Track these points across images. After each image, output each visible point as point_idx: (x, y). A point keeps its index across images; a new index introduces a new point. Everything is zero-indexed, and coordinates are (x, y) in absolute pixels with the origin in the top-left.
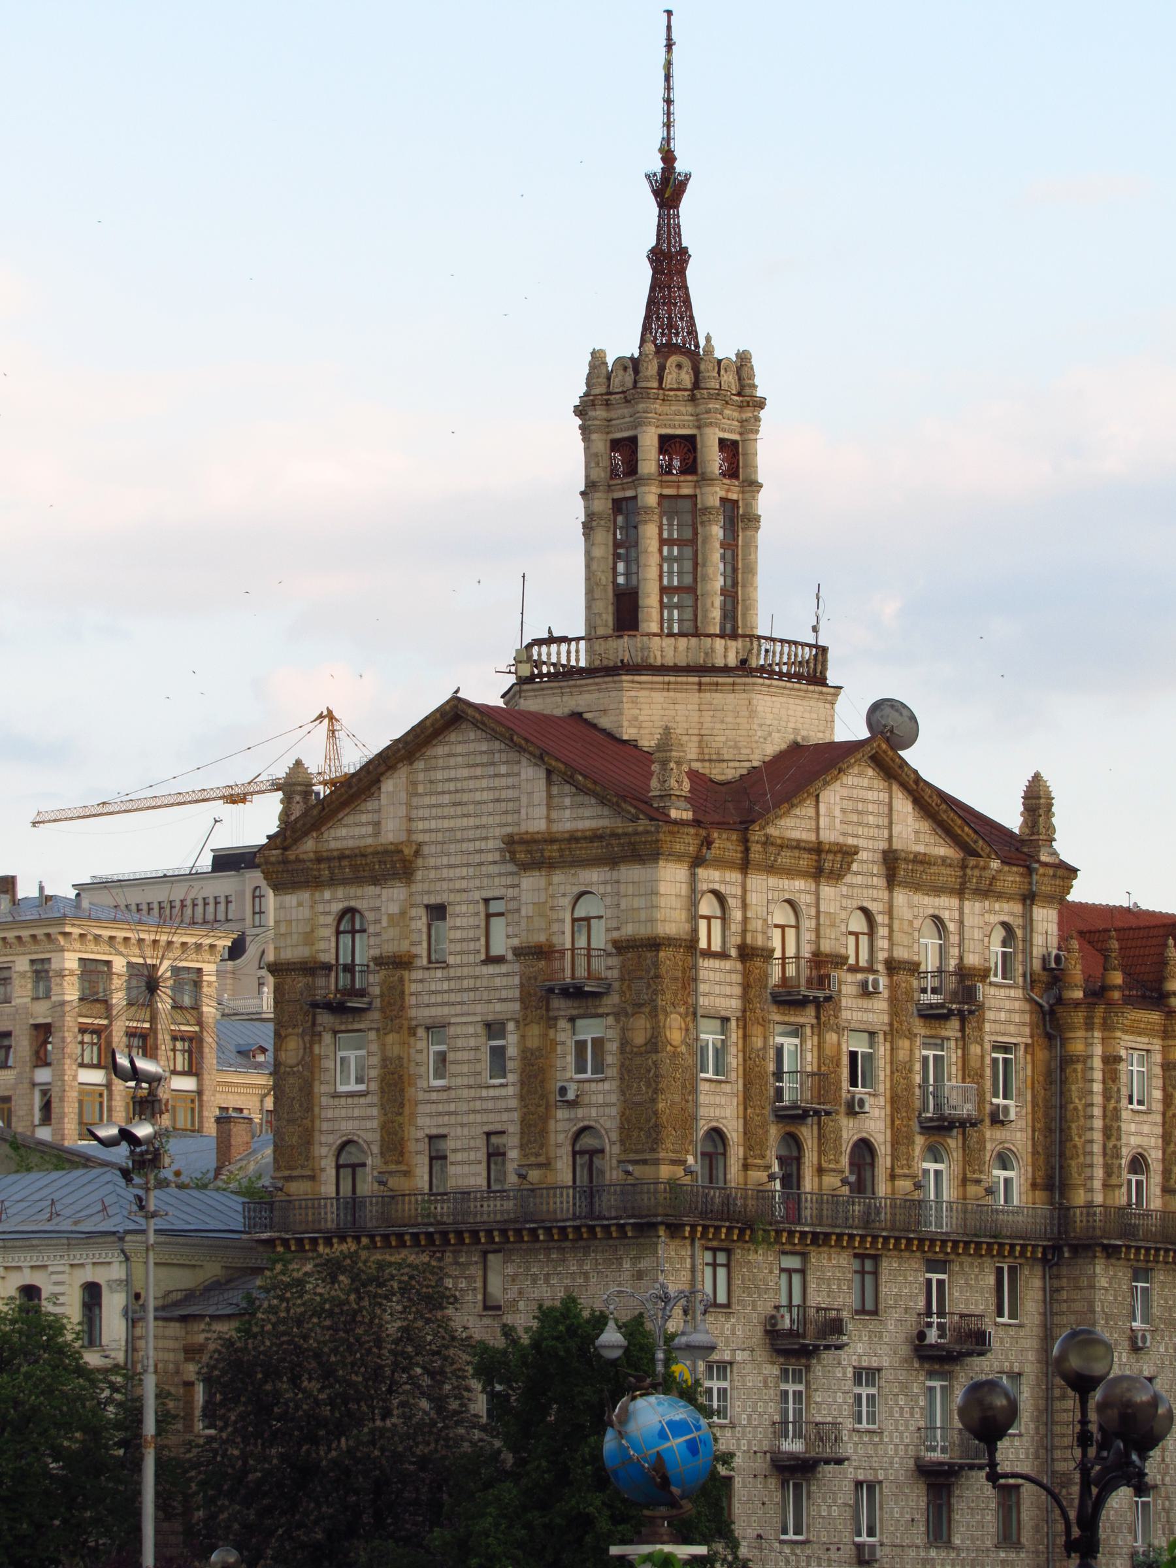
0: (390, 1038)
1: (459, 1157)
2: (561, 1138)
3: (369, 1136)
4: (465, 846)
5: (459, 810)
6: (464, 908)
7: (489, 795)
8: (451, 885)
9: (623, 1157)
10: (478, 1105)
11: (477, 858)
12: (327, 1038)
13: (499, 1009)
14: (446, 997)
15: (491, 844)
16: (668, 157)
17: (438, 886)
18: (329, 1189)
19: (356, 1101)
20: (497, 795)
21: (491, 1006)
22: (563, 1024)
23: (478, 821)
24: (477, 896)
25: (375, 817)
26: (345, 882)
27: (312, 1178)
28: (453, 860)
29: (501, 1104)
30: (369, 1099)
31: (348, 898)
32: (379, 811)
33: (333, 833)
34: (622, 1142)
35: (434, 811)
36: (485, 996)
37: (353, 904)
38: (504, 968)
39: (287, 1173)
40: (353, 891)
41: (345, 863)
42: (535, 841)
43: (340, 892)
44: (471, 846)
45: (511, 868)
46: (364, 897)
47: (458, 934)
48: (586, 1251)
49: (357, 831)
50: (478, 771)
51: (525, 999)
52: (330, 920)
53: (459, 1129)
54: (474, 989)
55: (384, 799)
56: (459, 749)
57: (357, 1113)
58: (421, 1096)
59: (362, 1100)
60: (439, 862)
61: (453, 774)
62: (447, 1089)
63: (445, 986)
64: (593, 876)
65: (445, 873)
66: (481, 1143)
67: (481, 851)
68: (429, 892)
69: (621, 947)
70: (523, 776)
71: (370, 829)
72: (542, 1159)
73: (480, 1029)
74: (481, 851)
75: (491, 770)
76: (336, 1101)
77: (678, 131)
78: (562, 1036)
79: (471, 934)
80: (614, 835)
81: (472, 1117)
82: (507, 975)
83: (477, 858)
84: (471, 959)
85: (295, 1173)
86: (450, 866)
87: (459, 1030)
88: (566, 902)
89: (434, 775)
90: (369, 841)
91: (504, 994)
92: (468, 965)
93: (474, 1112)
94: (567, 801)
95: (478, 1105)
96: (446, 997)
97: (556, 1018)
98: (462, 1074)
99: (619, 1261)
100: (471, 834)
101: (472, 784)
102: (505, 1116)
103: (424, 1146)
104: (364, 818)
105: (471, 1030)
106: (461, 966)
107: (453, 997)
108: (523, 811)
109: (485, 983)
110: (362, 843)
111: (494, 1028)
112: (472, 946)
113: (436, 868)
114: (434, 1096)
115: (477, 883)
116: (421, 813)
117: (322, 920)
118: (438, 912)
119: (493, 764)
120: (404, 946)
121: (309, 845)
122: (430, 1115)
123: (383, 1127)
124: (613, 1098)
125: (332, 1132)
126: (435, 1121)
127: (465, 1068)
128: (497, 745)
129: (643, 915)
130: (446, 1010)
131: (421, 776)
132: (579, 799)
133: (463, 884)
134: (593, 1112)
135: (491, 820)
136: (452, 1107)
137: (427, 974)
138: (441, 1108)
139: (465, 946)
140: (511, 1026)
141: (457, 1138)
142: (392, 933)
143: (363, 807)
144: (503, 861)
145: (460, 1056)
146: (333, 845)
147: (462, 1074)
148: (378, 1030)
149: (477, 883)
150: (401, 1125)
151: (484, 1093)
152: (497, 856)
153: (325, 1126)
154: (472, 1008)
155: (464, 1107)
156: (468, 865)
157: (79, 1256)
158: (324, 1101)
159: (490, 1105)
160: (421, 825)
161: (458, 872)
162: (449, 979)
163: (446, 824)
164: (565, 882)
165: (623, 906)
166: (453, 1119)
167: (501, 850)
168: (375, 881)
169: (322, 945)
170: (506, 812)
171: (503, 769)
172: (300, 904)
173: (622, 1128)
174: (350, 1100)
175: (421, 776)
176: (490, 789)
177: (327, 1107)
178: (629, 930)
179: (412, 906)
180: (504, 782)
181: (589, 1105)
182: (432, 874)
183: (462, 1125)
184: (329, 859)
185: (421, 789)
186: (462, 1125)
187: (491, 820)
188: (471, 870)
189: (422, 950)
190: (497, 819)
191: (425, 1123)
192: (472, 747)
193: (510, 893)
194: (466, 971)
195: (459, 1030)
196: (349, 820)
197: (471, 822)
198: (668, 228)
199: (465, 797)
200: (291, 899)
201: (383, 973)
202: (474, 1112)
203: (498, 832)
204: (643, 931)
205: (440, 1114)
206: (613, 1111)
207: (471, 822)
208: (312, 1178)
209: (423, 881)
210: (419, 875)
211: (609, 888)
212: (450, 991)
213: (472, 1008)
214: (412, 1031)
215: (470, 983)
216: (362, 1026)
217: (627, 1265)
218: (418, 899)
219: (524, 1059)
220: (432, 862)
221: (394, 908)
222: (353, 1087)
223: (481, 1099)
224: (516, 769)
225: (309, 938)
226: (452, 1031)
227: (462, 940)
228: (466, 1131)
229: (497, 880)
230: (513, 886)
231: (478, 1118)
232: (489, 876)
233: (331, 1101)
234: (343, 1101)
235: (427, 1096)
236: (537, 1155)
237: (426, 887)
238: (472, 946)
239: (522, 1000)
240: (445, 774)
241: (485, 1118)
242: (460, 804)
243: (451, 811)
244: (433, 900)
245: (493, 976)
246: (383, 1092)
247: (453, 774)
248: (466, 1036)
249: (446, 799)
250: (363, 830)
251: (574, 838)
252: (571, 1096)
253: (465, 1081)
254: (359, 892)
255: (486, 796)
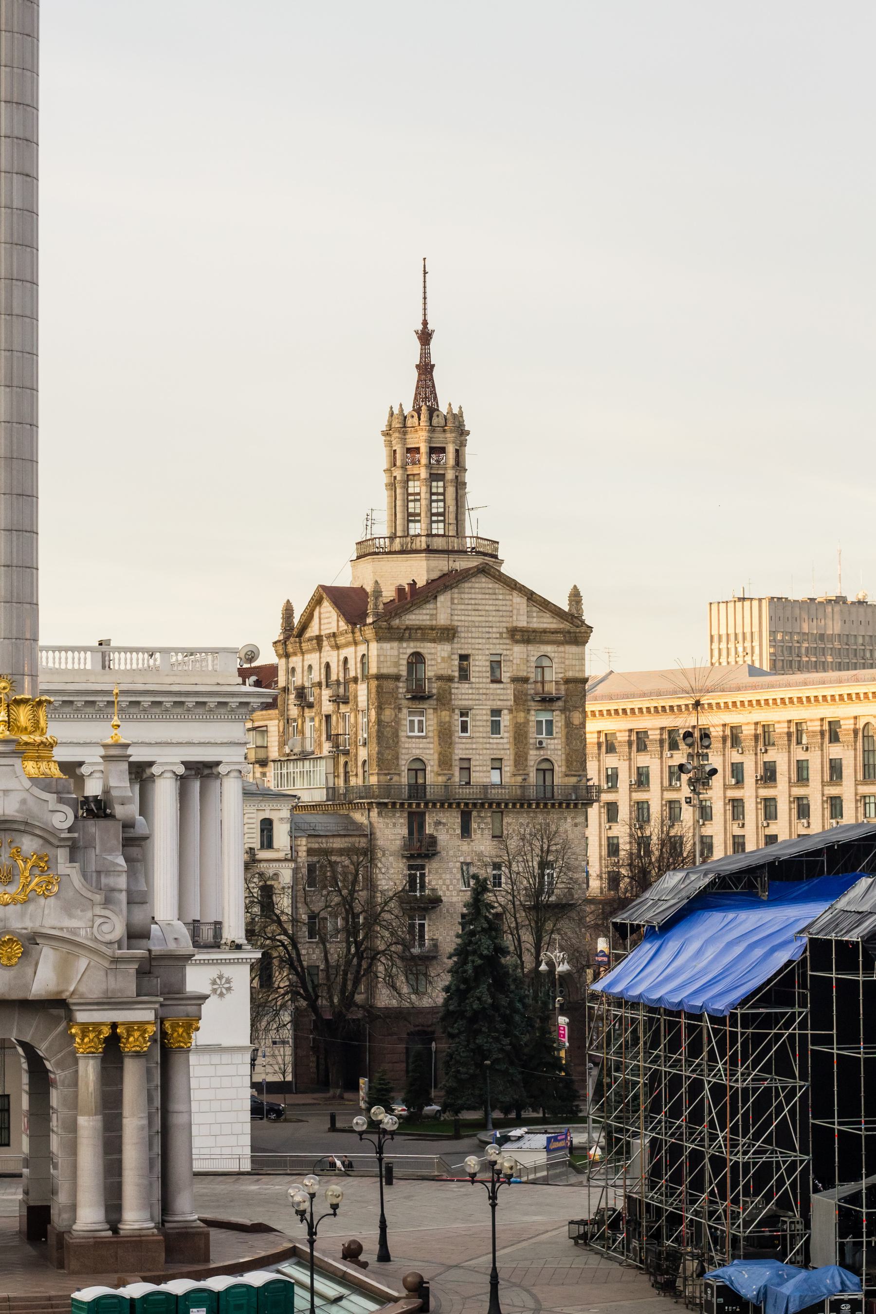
0: (444, 713)
1: (478, 768)
2: (532, 763)
3: (428, 757)
4: (480, 629)
5: (477, 613)
6: (480, 657)
7: (494, 608)
8: (473, 646)
9: (568, 773)
10: (488, 746)
11: (487, 635)
12: (405, 711)
13: (498, 704)
14: (470, 696)
15: (495, 630)
16: (425, 323)
17: (466, 646)
18: (404, 780)
19: (421, 740)
20: (497, 608)
21: (495, 703)
22: (533, 712)
23: (487, 619)
24: (487, 652)
25: (432, 612)
26: (417, 640)
27: (399, 775)
28: (474, 635)
29: (501, 746)
30: (428, 740)
31: (416, 647)
32: (436, 609)
33: (407, 617)
34: (568, 767)
35: (463, 612)
36: (492, 697)
37: (419, 650)
38: (501, 686)
39: (386, 772)
40: (418, 644)
41: (420, 631)
42: (528, 631)
43: (412, 644)
44: (484, 630)
45: (508, 641)
46: (427, 648)
47: (477, 669)
48: (548, 813)
49: (421, 617)
50: (487, 596)
51: (516, 698)
52: (406, 656)
53: (478, 757)
54: (486, 694)
55: (439, 604)
56: (477, 585)
57: (421, 746)
58: (457, 740)
59: (424, 740)
60: (466, 635)
61: (473, 596)
62: (470, 738)
63: (470, 691)
64: (548, 649)
65: (470, 640)
66: (489, 763)
67: (489, 633)
68: (461, 649)
69: (567, 681)
70: (515, 600)
71: (428, 617)
72: (525, 772)
73: (489, 712)
74: (489, 633)
75: (494, 597)
76: (410, 740)
77: (428, 312)
78: (533, 718)
79: (484, 669)
80: (569, 632)
81: (485, 751)
82: (503, 689)
83: (487, 635)
84: (484, 680)
85: (390, 772)
86: (472, 638)
87: (478, 712)
88: (535, 658)
89: (463, 596)
90: (428, 623)
91: (502, 697)
92: (483, 683)
93: (486, 749)
94: (535, 614)
95: (488, 746)
96: (470, 696)
97: (529, 710)
98: (479, 732)
99: (566, 819)
100: (484, 624)
101: (484, 602)
102: (502, 752)
103: (457, 763)
104: (424, 612)
105: (484, 712)
106: (479, 683)
107: (474, 697)
108: (515, 617)
109: (491, 691)
110: (424, 623)
111: (496, 712)
112: (484, 674)
113: (465, 638)
114: (464, 740)
115: (487, 646)
116: (456, 612)
117: (401, 656)
118: (464, 658)
119: (495, 594)
120: (450, 672)
121: (396, 622)
122: (462, 749)
123: (440, 754)
124: (560, 747)
125: (408, 754)
126: (464, 752)
127: (481, 729)
128: (497, 586)
129: (577, 668)
130: (470, 702)
131: (456, 596)
132: (541, 614)
133: (480, 646)
134: (549, 752)
135: (494, 619)
136: (474, 746)
137: (460, 685)
138: (467, 746)
139: (481, 675)
140: (505, 712)
141: (476, 760)
142: (443, 665)
143: (424, 606)
144: (501, 638)
145: (478, 723)
146: (407, 622)
147: (479, 732)
148: (434, 709)
149: (487, 646)
150: (450, 753)
151: (491, 741)
152: (498, 636)
153: (404, 751)
154: (484, 702)
155: (481, 746)
156: (482, 638)
157: (263, 806)
158: (403, 739)
159: (495, 746)
160: (456, 618)
161: (477, 641)
162: (472, 688)
163: (470, 618)
164: (535, 651)
165: (567, 662)
166: (474, 752)
167: (501, 633)
168: (434, 641)
169: (402, 668)
170: (502, 616)
171: (501, 597)
172: (392, 648)
173: (567, 761)
174: (417, 740)
175: (456, 596)
176: (492, 605)
177: (405, 742)
178: (570, 674)
179: (452, 654)
180: (500, 602)
181: (547, 749)
182: (463, 640)
183: (479, 754)
184: (410, 629)
185: (456, 601)
186: (479, 754)
187: (494, 619)
188: (484, 641)
189: (456, 674)
190: (497, 619)
191: (459, 752)
192: (484, 585)
193: (505, 652)
194: (481, 686)
195: (478, 712)
196: (417, 612)
197: (483, 619)
198: (425, 355)
199: (480, 608)
200: (387, 646)
201: (439, 683)
202: (486, 749)
203: (504, 625)
204: (578, 675)
205: (467, 749)
206: (559, 753)
207: (483, 619)
208: (399, 775)
209: (458, 643)
210: (456, 640)
211: (556, 655)
212: (472, 694)
213: (484, 702)
214: (453, 710)
215: (484, 691)
216: (425, 706)
217: (569, 820)
218: (455, 651)
219: (515, 726)
220: (463, 635)
221: (445, 654)
222: (416, 734)
223: (490, 743)
224: (507, 597)
225: (397, 664)
226: (473, 712)
227: (479, 672)
228: (481, 757)
229: (498, 646)
230: (507, 650)
231: (488, 751)
232: (494, 644)
233: (407, 740)
234: (414, 740)
235: (460, 740)
236: (524, 770)
237: (459, 646)
238: (484, 674)
239: (515, 701)
240: (470, 596)
241: (492, 752)
242: (477, 610)
243: (473, 613)
244: (463, 652)
245: (496, 689)
246: (439, 737)
247: (473, 596)
248: (481, 715)
249: (470, 607)
250: (425, 617)
251: (545, 631)
252: (544, 745)
253: (481, 735)
254: (422, 645)
255: (491, 608)
